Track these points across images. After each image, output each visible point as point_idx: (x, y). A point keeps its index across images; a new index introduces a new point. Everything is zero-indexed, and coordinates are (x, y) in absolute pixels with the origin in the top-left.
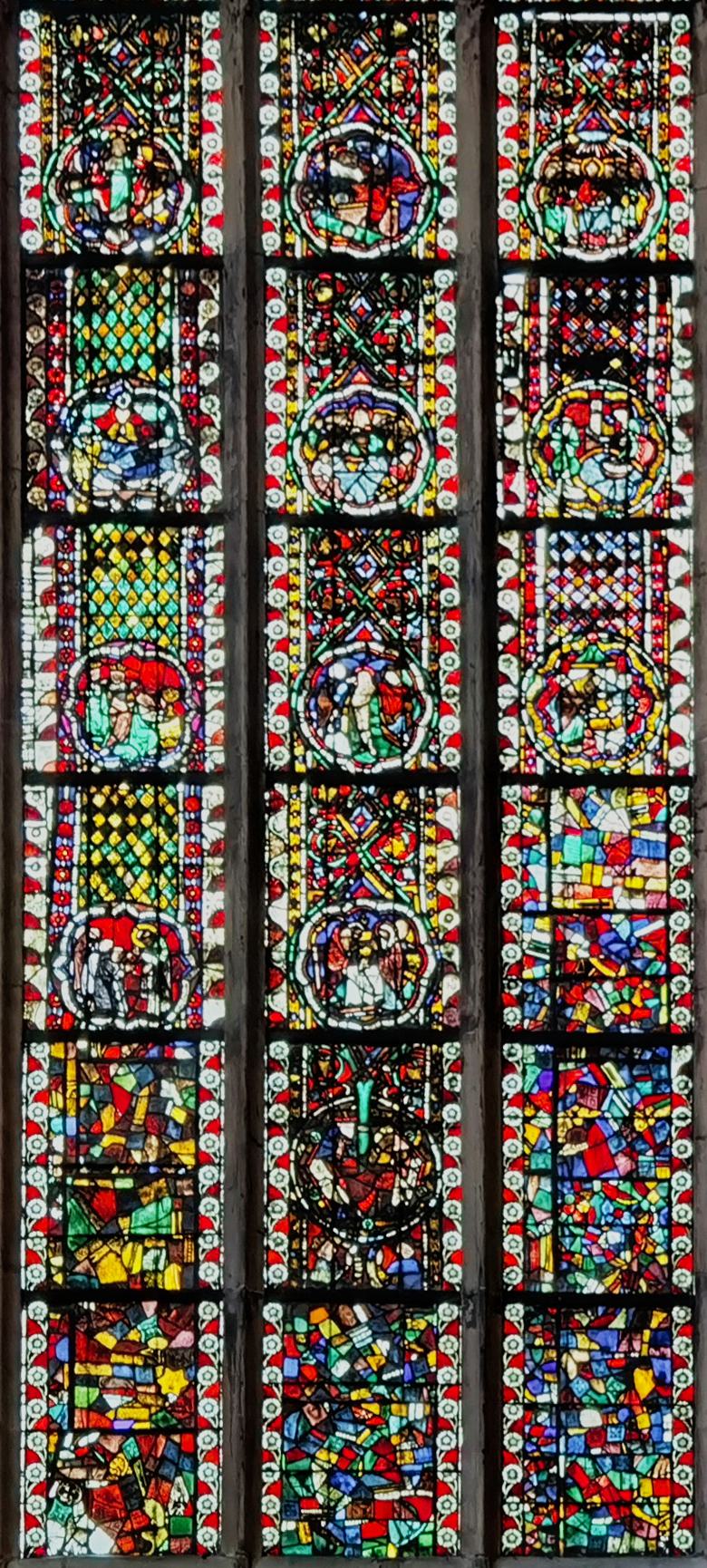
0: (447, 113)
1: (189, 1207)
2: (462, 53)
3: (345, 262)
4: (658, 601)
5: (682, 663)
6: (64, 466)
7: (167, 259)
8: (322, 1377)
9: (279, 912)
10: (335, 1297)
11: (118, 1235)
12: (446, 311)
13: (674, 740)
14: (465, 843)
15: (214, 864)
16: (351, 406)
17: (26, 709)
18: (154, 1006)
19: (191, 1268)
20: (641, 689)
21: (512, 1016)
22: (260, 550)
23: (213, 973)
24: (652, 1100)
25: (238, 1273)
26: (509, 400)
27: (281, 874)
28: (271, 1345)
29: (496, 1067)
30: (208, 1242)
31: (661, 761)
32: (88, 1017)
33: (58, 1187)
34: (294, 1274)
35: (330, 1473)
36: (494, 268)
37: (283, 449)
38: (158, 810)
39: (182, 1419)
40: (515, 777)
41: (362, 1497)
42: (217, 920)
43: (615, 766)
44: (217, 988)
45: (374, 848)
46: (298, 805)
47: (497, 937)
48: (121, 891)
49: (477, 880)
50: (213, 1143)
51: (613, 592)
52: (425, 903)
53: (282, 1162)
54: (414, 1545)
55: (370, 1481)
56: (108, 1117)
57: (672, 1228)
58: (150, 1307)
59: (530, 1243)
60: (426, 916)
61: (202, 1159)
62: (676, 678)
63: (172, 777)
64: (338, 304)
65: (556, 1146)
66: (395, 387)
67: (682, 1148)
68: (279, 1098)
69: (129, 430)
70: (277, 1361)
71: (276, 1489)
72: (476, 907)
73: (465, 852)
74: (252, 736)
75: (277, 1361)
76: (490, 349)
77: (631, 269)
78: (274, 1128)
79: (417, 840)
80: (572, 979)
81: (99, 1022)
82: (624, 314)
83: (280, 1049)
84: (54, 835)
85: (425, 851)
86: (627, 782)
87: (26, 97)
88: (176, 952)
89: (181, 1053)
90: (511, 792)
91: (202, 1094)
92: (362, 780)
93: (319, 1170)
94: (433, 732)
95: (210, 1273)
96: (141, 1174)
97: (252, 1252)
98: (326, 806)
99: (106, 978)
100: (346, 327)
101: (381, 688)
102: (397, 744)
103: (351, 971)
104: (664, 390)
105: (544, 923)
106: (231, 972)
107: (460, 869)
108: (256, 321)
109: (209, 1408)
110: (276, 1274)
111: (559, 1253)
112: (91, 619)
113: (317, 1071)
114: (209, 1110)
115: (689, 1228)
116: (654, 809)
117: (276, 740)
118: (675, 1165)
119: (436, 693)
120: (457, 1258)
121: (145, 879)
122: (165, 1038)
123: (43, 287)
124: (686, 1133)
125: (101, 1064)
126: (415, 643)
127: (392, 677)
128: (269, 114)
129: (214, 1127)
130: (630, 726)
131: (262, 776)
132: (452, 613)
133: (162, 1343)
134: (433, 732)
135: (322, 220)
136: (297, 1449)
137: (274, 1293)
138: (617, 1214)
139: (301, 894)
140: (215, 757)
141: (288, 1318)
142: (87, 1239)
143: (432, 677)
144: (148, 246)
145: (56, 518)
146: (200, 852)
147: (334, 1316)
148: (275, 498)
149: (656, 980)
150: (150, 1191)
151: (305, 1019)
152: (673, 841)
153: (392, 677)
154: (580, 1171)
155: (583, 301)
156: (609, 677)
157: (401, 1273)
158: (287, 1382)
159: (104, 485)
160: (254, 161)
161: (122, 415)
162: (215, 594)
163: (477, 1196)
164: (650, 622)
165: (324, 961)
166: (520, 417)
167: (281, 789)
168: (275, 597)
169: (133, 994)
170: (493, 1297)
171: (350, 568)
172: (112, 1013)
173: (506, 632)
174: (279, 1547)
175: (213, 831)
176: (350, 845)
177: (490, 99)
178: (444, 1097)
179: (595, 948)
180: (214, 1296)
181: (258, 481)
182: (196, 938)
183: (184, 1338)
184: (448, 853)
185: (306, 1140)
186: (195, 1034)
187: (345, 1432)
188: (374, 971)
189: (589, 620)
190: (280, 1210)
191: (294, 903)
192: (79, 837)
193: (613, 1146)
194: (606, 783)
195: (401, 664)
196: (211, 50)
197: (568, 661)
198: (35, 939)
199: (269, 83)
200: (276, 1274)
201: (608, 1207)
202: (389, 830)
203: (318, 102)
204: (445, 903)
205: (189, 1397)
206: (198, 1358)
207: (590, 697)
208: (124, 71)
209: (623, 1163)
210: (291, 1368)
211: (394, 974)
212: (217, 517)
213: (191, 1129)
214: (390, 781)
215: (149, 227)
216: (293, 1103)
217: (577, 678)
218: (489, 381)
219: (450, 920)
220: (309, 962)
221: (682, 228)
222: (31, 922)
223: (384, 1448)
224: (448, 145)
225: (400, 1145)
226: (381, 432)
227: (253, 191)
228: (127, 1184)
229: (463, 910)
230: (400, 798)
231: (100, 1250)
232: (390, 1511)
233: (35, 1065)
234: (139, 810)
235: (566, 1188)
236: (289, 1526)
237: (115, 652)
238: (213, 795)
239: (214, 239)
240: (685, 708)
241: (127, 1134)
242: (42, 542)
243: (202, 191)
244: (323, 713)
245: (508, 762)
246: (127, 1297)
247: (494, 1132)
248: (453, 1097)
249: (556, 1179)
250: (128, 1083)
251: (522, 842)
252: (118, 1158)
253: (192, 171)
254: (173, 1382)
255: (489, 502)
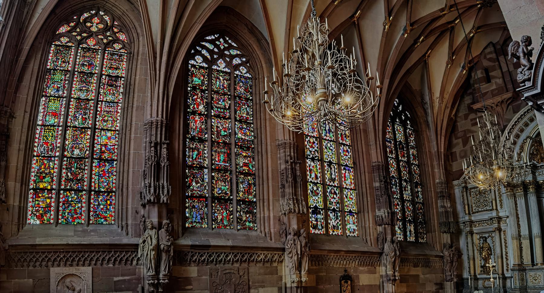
0: (98, 59)
1: (52, 178)
2: (101, 54)
3: (85, 72)
4: (116, 111)
5: (119, 118)
6: (48, 91)
7: (64, 70)
8: (68, 200)
9: (67, 142)
10: (70, 190)
11: (43, 182)
12: (95, 78)
13: (117, 126)
14: (91, 136)
15: (59, 136)
16: (83, 87)
17: (39, 117)
18: (50, 153)
19: (52, 186)
20: (114, 120)
21: (95, 156)
22: (70, 101)
23: (58, 149)
24: (111, 167)
25: (58, 187)
26: (102, 88)
27: (68, 138)
28: (61, 196)
29: (92, 162)
30: (54, 183)
31: (115, 128)
32: (42, 154)
33: (36, 175)
34: (65, 187)
35: (68, 213)
36: (101, 75)
37: (74, 91)
38: (53, 130)
39: (49, 206)
40: (98, 129)
41: (72, 216)
42: (59, 143)
43: (110, 128)
44: (58, 151)
45: (80, 136)
46: (70, 130)
47: (94, 147)
48: (47, 139)
49: (92, 140)
50: (56, 170)
51: (111, 109)
52: (85, 142)
53: (64, 173)
54: (78, 223)
55: (73, 214)
56: (43, 167)
57: (113, 183)
58: (46, 191)
59: (95, 184)
60: (85, 144)
61: (54, 172)
62: (118, 119)
63: (55, 126)
64: (83, 76)
65: (99, 172)
66: (88, 85)
67: (115, 173)
68: (65, 165)
69: (56, 87)
70: (62, 198)
71: (61, 215)
72: (91, 143)
73: (91, 137)
74: (66, 122)
75: (62, 198)
76: (100, 83)
77: (117, 77)
78: (64, 169)
79: (85, 135)
80: (102, 152)
81: (43, 155)
82: (116, 81)
83: (65, 159)
84: (40, 132)
85: (86, 136)
86: (111, 130)
87: (51, 53)
88: (53, 147)
89: (53, 159)
90: (97, 130)
91: (55, 164)
92: (79, 128)
93: (69, 174)
94: (88, 123)
95: (54, 187)
96: (46, 174)
97: (60, 184)
98: (74, 130)
99: (44, 149)
100: (83, 79)
101: (82, 117)
102: (84, 124)
103: (75, 150)
104: (120, 89)
105: (100, 146)
106: (60, 149)
107: (90, 139)
108: (73, 77)
109: (53, 204)
110: (63, 187)
111: (99, 186)
112: (48, 107)
113: (70, 162)
114: (56, 166)
115: (115, 183)
116: (114, 134)
117: (69, 122)
118: (114, 175)
119: (89, 119)
120: (86, 186)
121: (51, 138)
122: (51, 157)
123: (49, 72)
124: (115, 172)
125: (43, 160)
126: (87, 113)
127: (84, 116)
128: (78, 57)
129: (56, 168)
130: (112, 124)
131: (67, 126)
132: (92, 110)
133: (47, 196)
134: (88, 123)
135: (82, 68)
136: (64, 210)
137: (62, 189)
138: (106, 181)
139: (70, 140)
140: (61, 124)
141: (64, 193)
142: (39, 182)
143: (89, 117)
144: (62, 69)
145: (46, 96)
146: (58, 135)
147: (70, 193)
148: (72, 96)
149: (113, 153)
150: (47, 176)
151: (69, 155)
152: (116, 137)
153: (84, 116)
154: (102, 176)
155: (111, 79)
156: (110, 118)
157: (78, 187)
158: (63, 201)
159: (52, 93)
160: (76, 61)
161: (56, 86)
162: (64, 106)
163: (89, 178)
164: (115, 113)
165: (72, 149)
166: (103, 90)
167: (69, 128)
168: (71, 106)
169: (48, 152)
170: (90, 191)
171: (80, 104)
172: (45, 154)
173: (98, 113)
174: (61, 223)
175: (60, 132)
176: (76, 135)
177: (104, 58)
178: (86, 166)
179: (106, 149)
180: (54, 190)
181: (71, 94)
182: (56, 145)
183: (50, 195)
184: (88, 137)
185: (68, 170)
186: (55, 157)
187: (70, 208)
188: (78, 150)
189: (108, 112)
190: (64, 179)
191: (69, 141)
192: (43, 132)
193: (106, 173)
194: (108, 130)
195: (85, 115)
196: (73, 51)
197: (105, 116)
198: (36, 144)
199: (79, 54)
200: (63, 187)
201: (105, 180)
202: (82, 134)
203: (84, 57)
204: (88, 142)
205: (50, 203)
206: (52, 198)
207: (107, 121)
208: (62, 51)
209: (107, 175)
210: (64, 199)
211: (81, 151)
212: (65, 97)
213: (53, 168)
214: (82, 128)
215: (62, 67)
216: (66, 166)
217: (106, 118)
218: (99, 86)
219: (88, 145)
220: (70, 148)
221: (124, 74)
222: (36, 142)
223: (75, 210)
224: (98, 62)
225: (79, 171)
226: (86, 90)
227: (75, 64)
228: (44, 175)
229: (90, 144)
230: (83, 130)
231: (40, 183)
232: (75, 218)
233: (34, 160)
234: (51, 129)
235: (100, 178)
236: (62, 220)
237: (51, 111)
238: (60, 128)
239: (70, 69)
240: (119, 123)
241: (45, 169)
242: (44, 99)
243: (69, 64)
244: (75, 120)
245: (97, 127)
246: (43, 190)
247: (91, 170)
248: (87, 166)
249: (99, 176)
250: (46, 162)
251: (98, 136)
252: (44, 172)
253: (68, 62)
254: (48, 201)
255: (98, 98)
